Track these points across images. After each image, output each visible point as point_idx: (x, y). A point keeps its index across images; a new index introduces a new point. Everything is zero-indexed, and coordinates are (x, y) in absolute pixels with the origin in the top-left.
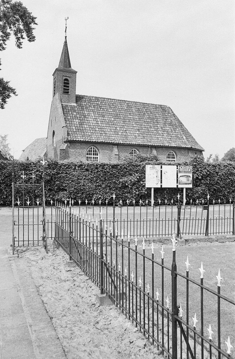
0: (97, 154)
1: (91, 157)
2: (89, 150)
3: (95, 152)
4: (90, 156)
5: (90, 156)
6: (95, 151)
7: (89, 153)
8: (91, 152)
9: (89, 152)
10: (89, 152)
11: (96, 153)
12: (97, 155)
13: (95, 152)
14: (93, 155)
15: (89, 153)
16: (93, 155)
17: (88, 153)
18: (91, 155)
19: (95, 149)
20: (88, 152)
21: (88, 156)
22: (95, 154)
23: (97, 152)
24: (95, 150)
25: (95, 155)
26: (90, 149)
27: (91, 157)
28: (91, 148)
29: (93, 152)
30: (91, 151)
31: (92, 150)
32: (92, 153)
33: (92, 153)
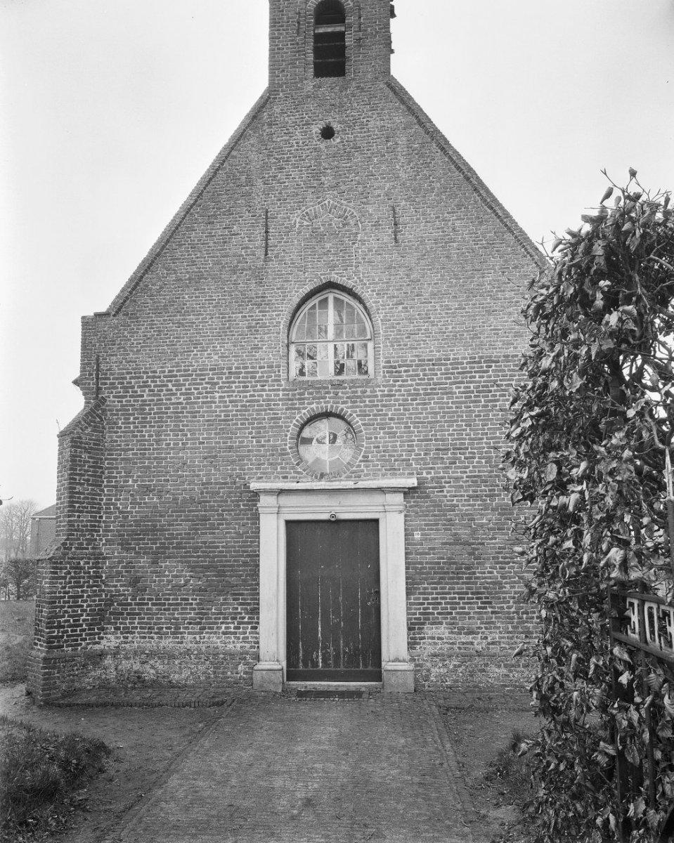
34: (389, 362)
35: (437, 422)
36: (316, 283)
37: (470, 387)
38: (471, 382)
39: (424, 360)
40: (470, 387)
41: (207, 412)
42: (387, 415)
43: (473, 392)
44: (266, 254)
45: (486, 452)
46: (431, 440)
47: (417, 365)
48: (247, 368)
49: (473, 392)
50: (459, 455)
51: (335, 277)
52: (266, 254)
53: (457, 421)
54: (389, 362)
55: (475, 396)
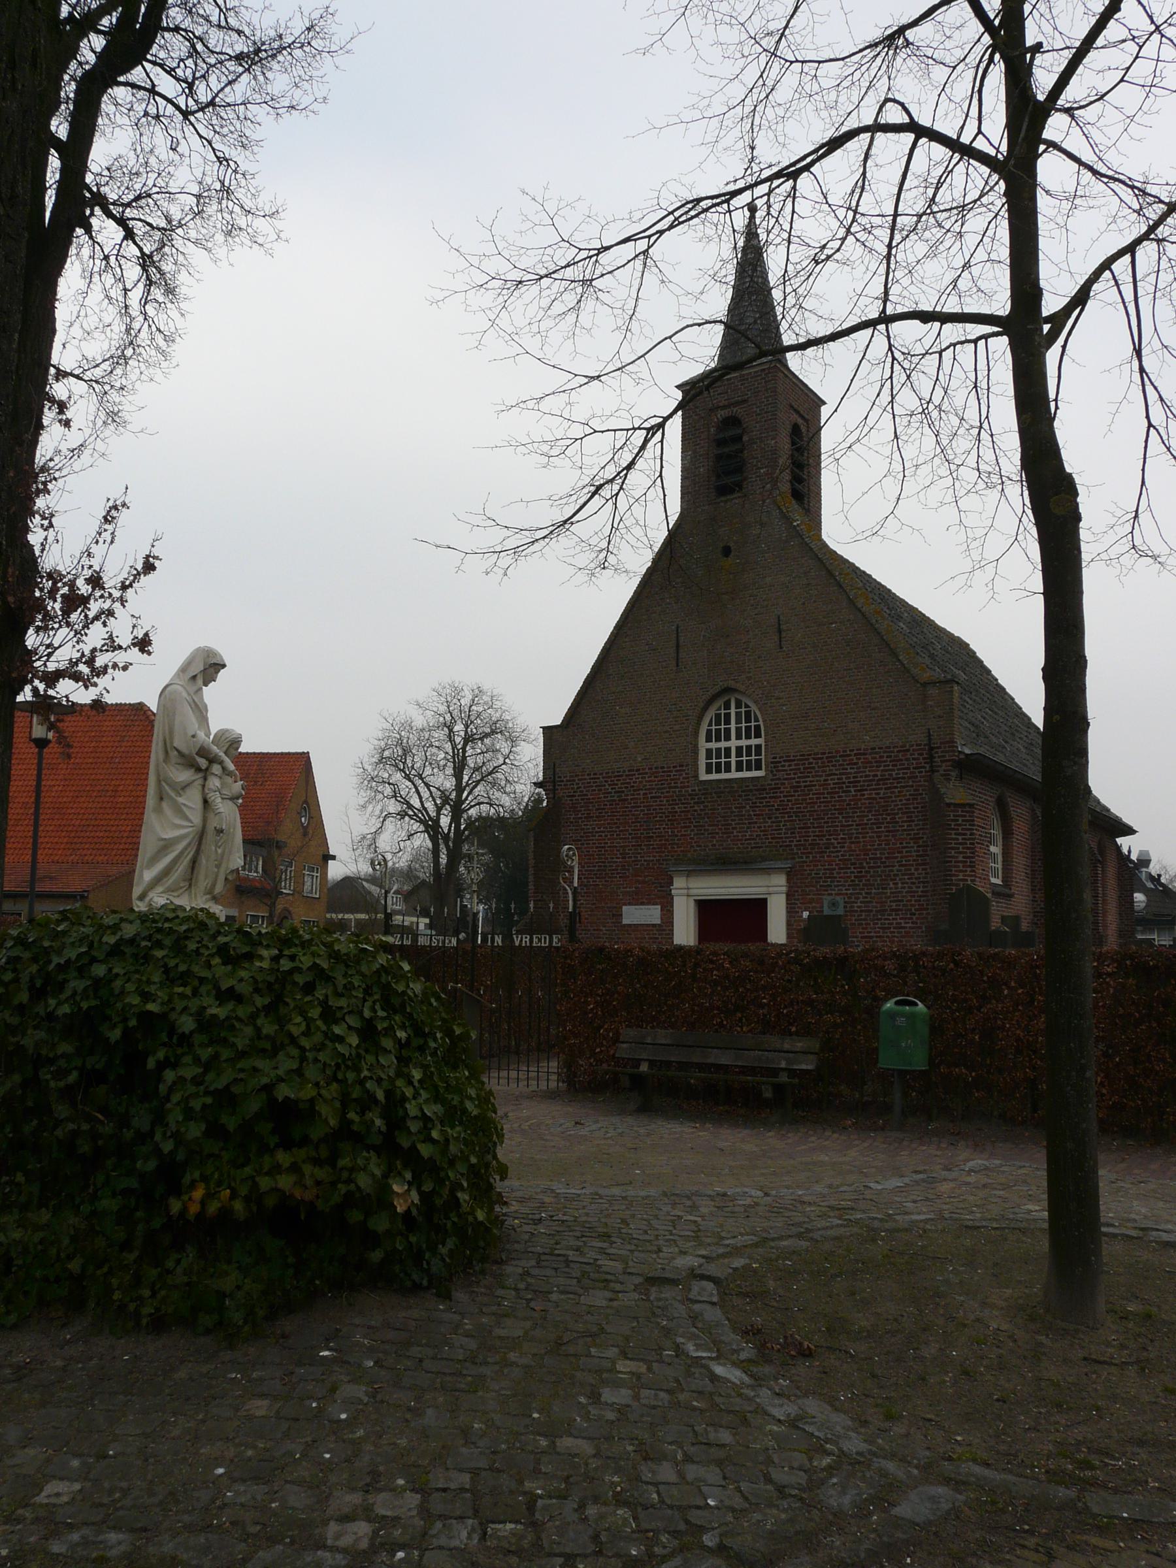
0: (757, 728)
1: (728, 750)
2: (718, 716)
3: (748, 720)
4: (723, 744)
5: (723, 744)
6: (748, 714)
7: (718, 731)
8: (728, 722)
9: (718, 723)
10: (718, 723)
11: (753, 724)
12: (758, 735)
13: (748, 720)
14: (739, 737)
15: (718, 731)
16: (739, 737)
17: (714, 727)
18: (728, 738)
19: (747, 706)
20: (710, 724)
21: (713, 745)
22: (748, 729)
23: (757, 720)
24: (743, 710)
25: (748, 737)
26: (719, 709)
27: (728, 750)
28: (727, 706)
29: (738, 721)
30: (728, 716)
31: (733, 711)
32: (733, 726)
33: (733, 726)
34: (775, 758)
35: (815, 811)
36: (717, 689)
37: (842, 779)
38: (843, 774)
39: (803, 755)
40: (842, 779)
41: (633, 807)
42: (773, 806)
43: (844, 783)
44: (677, 666)
45: (856, 838)
46: (809, 828)
47: (798, 760)
48: (663, 768)
49: (844, 783)
50: (833, 841)
51: (731, 684)
52: (677, 666)
53: (831, 810)
54: (775, 758)
55: (847, 787)
